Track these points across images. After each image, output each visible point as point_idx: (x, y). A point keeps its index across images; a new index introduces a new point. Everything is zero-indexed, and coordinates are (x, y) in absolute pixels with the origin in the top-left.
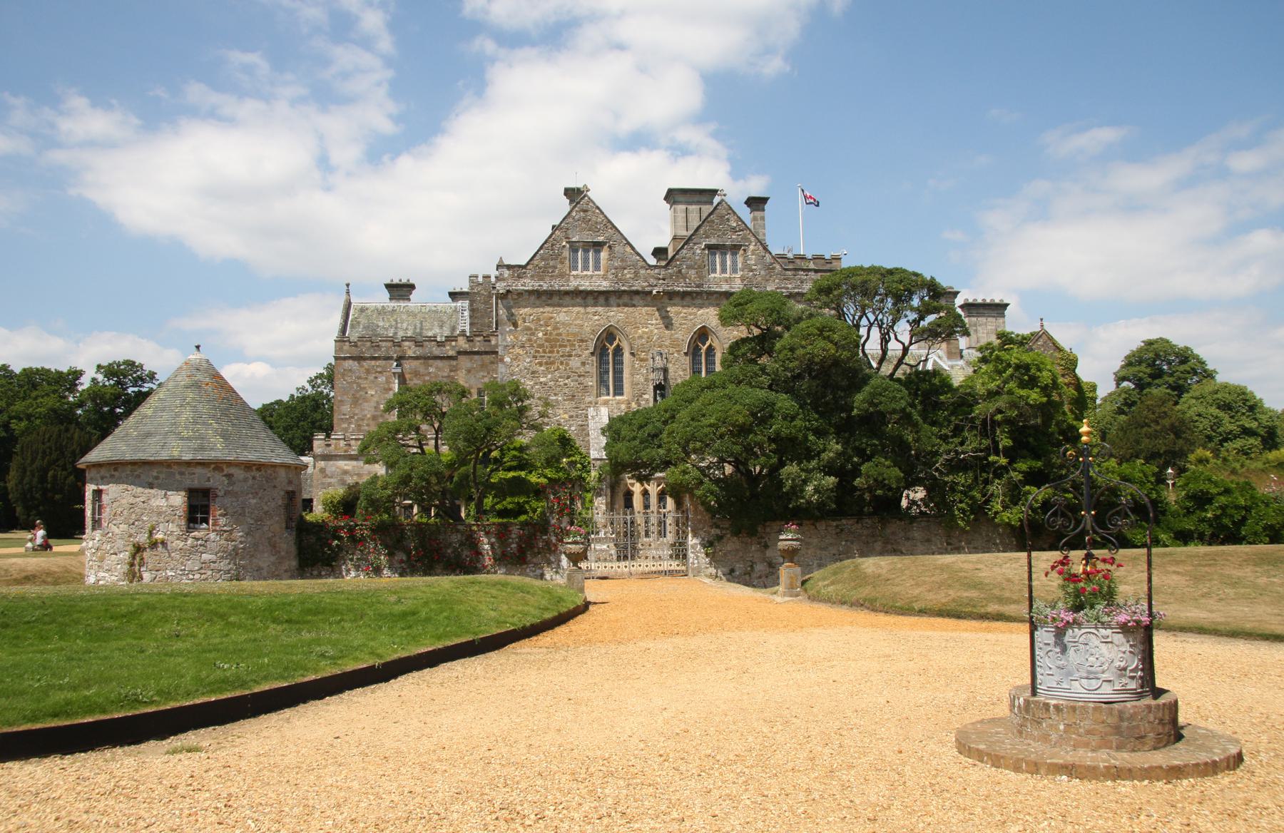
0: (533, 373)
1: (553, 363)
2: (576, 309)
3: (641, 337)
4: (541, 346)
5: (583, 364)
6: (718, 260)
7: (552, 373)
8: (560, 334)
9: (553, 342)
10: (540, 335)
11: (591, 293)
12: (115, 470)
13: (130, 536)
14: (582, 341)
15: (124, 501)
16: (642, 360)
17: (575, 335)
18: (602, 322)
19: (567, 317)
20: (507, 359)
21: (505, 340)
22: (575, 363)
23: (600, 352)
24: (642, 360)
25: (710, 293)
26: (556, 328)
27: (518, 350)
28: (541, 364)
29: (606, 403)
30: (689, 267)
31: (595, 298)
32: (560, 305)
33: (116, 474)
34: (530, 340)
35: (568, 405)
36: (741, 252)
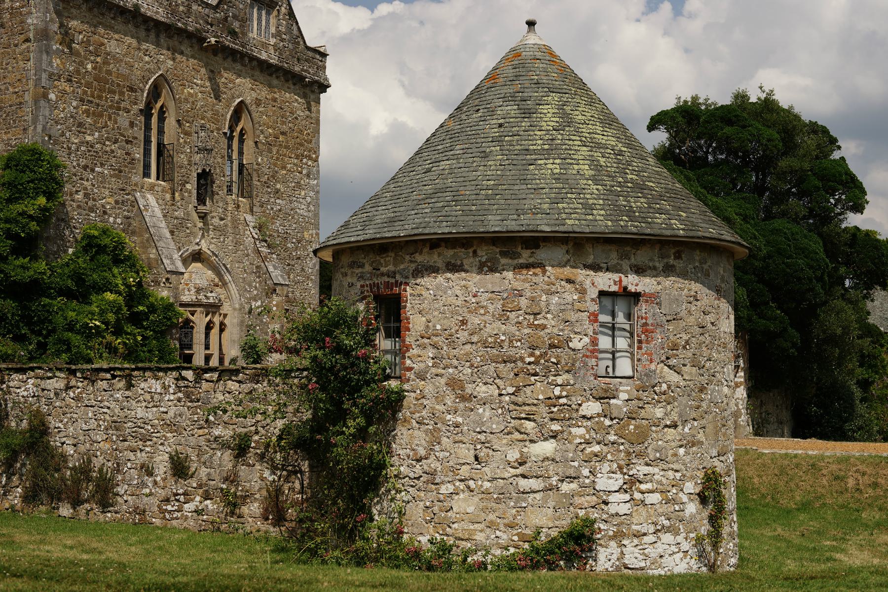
0: (80, 125)
1: (101, 116)
2: (129, 40)
3: (186, 100)
4: (89, 85)
5: (132, 124)
6: (264, 18)
7: (99, 130)
8: (109, 72)
9: (102, 83)
10: (89, 66)
11: (147, 20)
12: (678, 256)
13: (702, 390)
14: (132, 89)
15: (691, 320)
16: (187, 134)
17: (126, 78)
18: (152, 66)
19: (118, 44)
20: (52, 96)
21: (50, 63)
22: (123, 120)
23: (147, 113)
24: (187, 134)
25: (253, 59)
26: (106, 62)
27: (63, 85)
28: (87, 112)
29: (152, 188)
30: (235, 17)
31: (148, 30)
32: (112, 28)
33: (679, 264)
34: (78, 72)
35: (114, 183)
36: (275, 13)
